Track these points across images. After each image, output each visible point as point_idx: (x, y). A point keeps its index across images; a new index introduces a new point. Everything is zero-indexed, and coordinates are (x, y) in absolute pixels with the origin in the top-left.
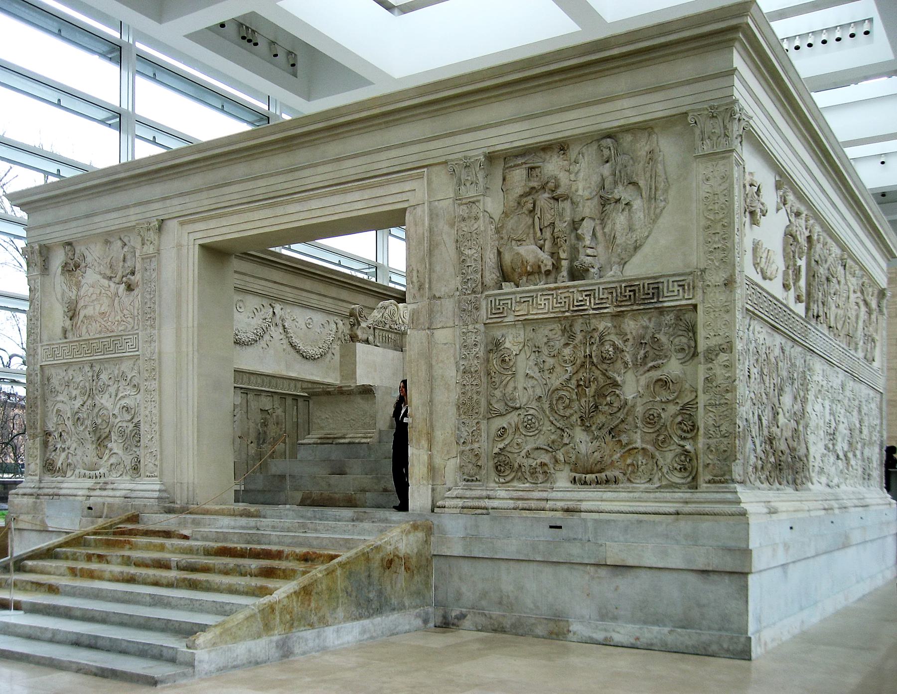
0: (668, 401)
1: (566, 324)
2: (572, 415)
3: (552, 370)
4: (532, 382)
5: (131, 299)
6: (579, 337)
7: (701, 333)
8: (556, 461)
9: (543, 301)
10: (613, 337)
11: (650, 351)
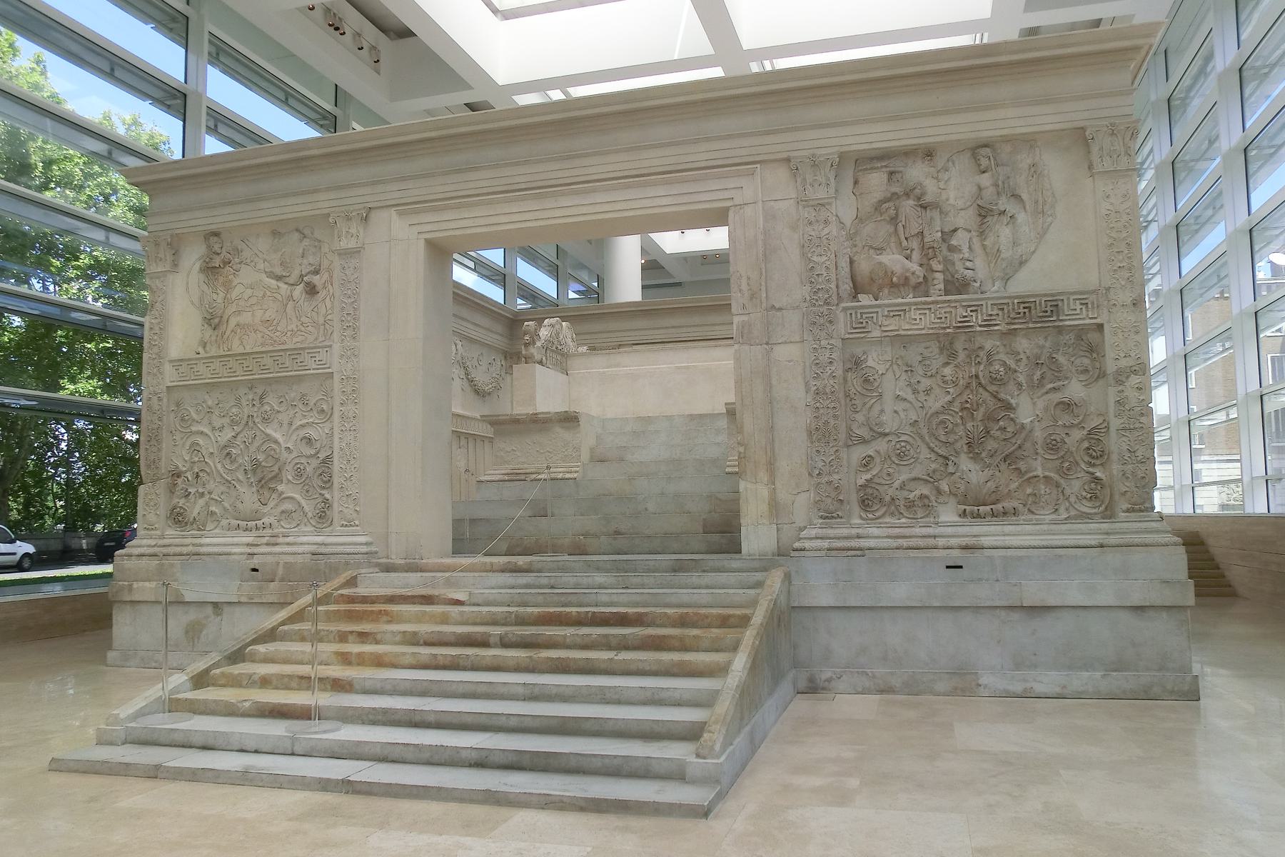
0: (1073, 426)
1: (946, 344)
2: (956, 441)
3: (928, 392)
4: (900, 406)
5: (314, 304)
6: (962, 356)
7: (1110, 354)
8: (939, 492)
10: (1002, 356)
11: (1047, 372)
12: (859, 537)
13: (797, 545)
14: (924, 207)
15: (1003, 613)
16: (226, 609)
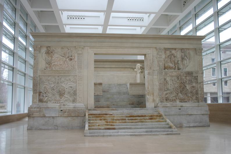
3: (175, 84)
5: (71, 62)
6: (180, 79)
7: (199, 80)
8: (177, 98)
9: (175, 73)
11: (191, 82)
12: (166, 105)
13: (158, 106)
14: (174, 57)
16: (55, 117)
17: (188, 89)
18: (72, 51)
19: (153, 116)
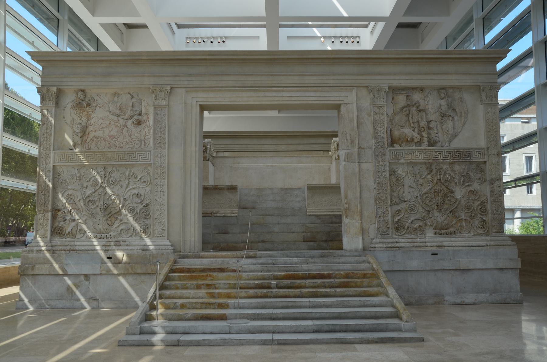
1: (429, 165)
3: (422, 185)
4: (411, 190)
5: (139, 130)
8: (426, 224)
11: (466, 179)
12: (397, 242)
13: (373, 246)
14: (419, 111)
15: (453, 272)
17: (458, 197)
18: (141, 100)
19: (352, 278)
